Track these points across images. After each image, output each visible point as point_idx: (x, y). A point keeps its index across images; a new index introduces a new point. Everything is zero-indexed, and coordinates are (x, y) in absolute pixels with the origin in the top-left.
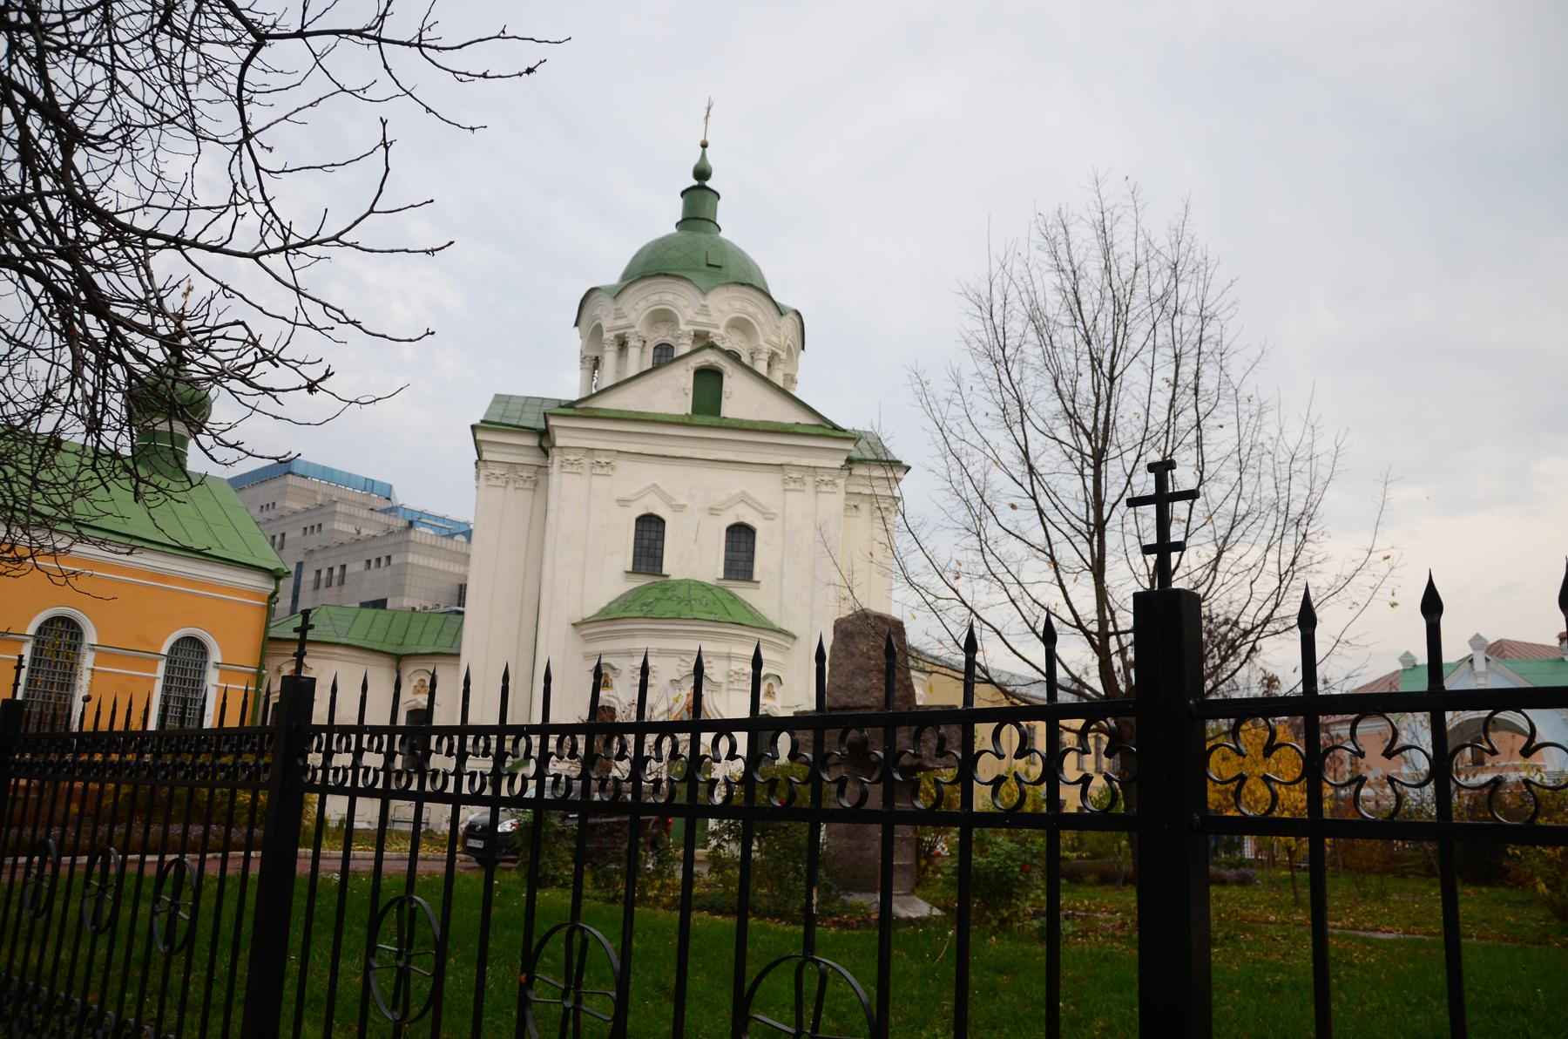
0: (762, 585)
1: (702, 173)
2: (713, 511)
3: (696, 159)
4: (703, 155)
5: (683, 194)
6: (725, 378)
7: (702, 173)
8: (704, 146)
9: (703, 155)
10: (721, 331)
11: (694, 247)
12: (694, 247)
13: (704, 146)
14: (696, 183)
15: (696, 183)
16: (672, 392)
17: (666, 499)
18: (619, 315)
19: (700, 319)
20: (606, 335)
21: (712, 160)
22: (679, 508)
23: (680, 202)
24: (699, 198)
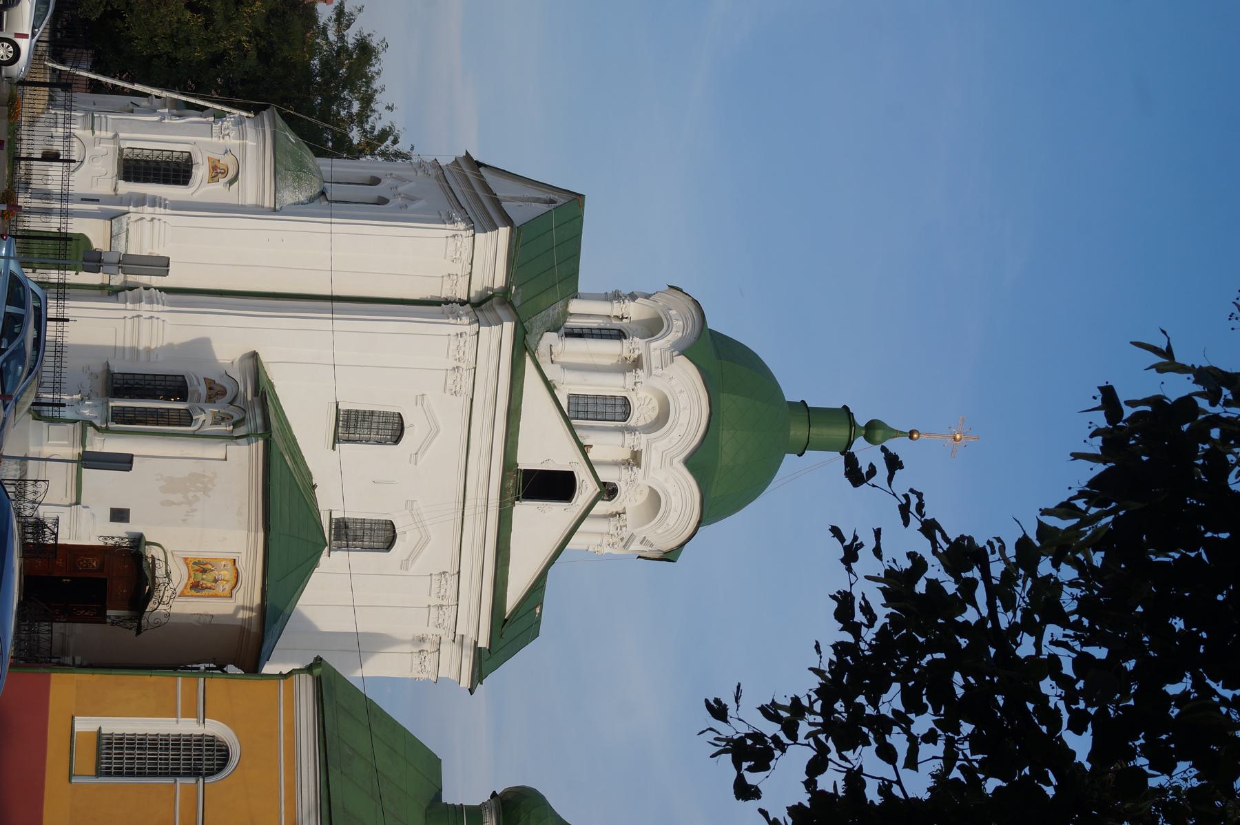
3: (891, 423)
4: (902, 434)
5: (845, 407)
9: (902, 434)
15: (861, 421)
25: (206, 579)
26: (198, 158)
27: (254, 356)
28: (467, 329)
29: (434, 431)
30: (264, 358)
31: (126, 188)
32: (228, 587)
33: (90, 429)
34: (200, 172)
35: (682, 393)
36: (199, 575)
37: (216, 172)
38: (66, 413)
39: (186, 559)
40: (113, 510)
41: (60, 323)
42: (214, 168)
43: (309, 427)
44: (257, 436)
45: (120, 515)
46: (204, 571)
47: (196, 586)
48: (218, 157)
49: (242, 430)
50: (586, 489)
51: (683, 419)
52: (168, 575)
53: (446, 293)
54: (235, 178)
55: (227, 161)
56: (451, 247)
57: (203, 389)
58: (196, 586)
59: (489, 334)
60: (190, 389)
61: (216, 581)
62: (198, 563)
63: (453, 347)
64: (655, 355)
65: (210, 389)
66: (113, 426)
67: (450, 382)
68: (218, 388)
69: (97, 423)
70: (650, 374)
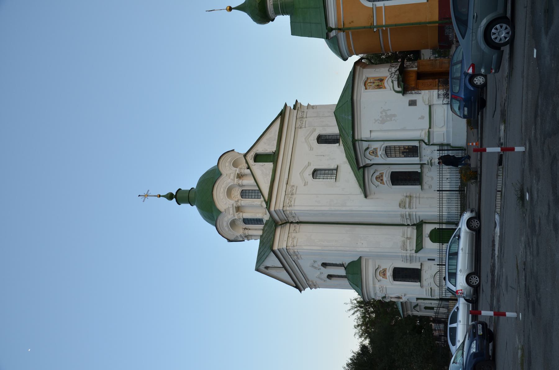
0: (338, 164)
1: (170, 197)
2: (311, 149)
4: (163, 196)
6: (258, 152)
7: (170, 197)
8: (160, 196)
9: (163, 196)
10: (238, 169)
11: (201, 196)
12: (201, 196)
13: (160, 196)
14: (174, 199)
15: (174, 199)
16: (263, 171)
17: (306, 168)
18: (227, 210)
19: (232, 177)
20: (236, 217)
21: (165, 194)
22: (309, 164)
23: (182, 205)
24: (180, 197)
25: (377, 83)
26: (391, 278)
27: (366, 196)
28: (288, 209)
29: (301, 173)
30: (363, 195)
31: (416, 266)
32: (369, 81)
33: (426, 141)
34: (389, 273)
35: (222, 200)
36: (380, 84)
37: (384, 273)
38: (437, 148)
39: (385, 88)
40: (416, 105)
41: (441, 189)
42: (384, 275)
43: (347, 173)
44: (358, 140)
45: (413, 103)
46: (378, 85)
47: (381, 80)
48: (384, 279)
49: (365, 145)
50: (250, 158)
51: (222, 190)
52: (392, 82)
53: (298, 226)
54: (376, 270)
55: (380, 278)
56: (295, 243)
57: (385, 179)
58: (381, 80)
59: (280, 207)
60: (390, 179)
61: (374, 83)
62: (380, 88)
63: (293, 202)
64: (231, 212)
65: (382, 180)
66: (416, 144)
67: (295, 190)
68: (379, 180)
69: (424, 144)
70: (233, 205)
